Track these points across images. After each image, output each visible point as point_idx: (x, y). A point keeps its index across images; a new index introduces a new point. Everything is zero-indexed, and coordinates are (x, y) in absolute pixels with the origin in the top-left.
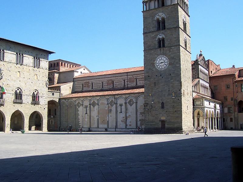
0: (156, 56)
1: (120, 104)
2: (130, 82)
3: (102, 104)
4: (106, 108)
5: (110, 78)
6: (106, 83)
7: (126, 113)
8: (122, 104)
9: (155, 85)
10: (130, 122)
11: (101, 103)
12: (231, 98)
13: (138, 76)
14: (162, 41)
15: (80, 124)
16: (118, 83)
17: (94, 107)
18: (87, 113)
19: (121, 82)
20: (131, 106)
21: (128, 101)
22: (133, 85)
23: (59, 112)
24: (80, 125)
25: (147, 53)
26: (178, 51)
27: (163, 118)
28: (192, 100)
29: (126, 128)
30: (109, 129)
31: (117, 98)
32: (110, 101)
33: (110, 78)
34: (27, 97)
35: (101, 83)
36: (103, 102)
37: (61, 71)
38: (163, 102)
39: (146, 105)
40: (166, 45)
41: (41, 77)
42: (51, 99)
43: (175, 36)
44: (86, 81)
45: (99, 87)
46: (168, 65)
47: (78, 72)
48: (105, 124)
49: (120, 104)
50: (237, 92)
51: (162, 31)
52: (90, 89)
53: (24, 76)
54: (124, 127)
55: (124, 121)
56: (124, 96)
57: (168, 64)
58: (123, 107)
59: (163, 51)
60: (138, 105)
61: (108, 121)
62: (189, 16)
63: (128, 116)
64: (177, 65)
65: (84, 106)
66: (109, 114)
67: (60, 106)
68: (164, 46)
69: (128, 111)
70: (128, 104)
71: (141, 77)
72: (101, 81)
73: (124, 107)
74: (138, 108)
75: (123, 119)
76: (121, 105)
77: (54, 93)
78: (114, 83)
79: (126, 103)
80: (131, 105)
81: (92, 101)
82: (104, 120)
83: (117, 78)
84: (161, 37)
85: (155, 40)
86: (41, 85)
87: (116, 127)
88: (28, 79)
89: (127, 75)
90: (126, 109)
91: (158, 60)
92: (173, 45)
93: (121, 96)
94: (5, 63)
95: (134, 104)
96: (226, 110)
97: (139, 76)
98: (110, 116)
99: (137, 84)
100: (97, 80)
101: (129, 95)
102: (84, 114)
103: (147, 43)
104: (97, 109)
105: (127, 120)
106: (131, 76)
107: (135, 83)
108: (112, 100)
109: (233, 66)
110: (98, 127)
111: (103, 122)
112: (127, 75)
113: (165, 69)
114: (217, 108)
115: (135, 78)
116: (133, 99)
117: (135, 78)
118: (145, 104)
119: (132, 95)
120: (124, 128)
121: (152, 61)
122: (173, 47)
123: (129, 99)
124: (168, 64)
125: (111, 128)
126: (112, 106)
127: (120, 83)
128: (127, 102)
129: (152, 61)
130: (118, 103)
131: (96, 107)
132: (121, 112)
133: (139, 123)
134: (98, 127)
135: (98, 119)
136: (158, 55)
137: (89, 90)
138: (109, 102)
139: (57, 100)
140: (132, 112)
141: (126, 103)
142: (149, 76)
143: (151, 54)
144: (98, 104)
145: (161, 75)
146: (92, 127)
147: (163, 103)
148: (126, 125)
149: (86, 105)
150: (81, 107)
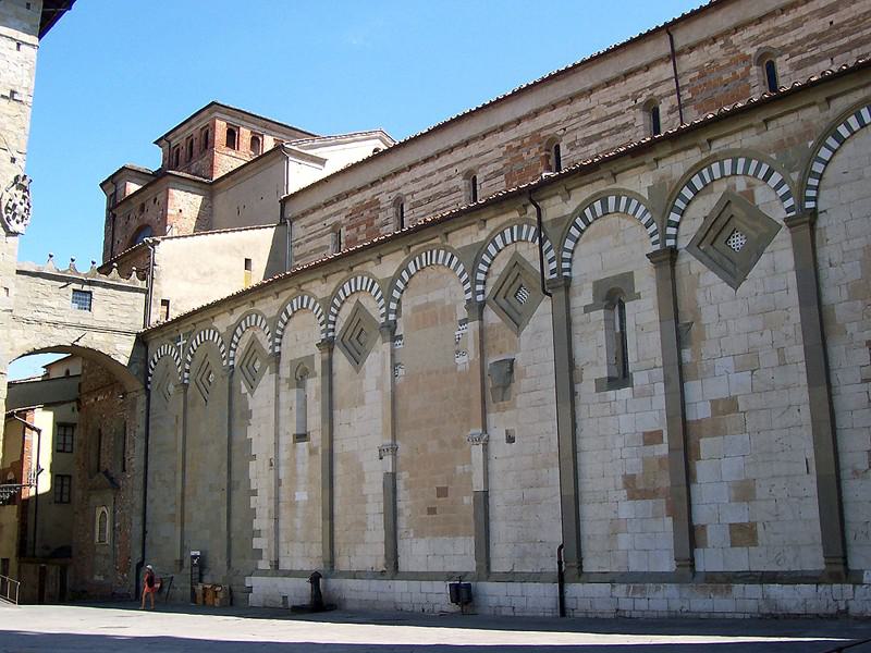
1: (597, 285)
3: (431, 316)
5: (528, 127)
7: (679, 375)
8: (628, 278)
10: (745, 492)
11: (416, 309)
17: (357, 359)
18: (301, 437)
19: (625, 127)
21: (691, 226)
23: (140, 444)
24: (257, 543)
30: (493, 593)
31: (566, 223)
32: (499, 267)
33: (528, 127)
35: (459, 182)
36: (434, 296)
42: (66, 337)
44: (358, 198)
48: (454, 533)
49: (597, 285)
54: (667, 565)
55: (664, 482)
56: (639, 181)
58: (643, 313)
60: (827, 253)
61: (484, 499)
63: (699, 411)
65: (285, 371)
66: (492, 417)
67: (148, 392)
69: (709, 349)
70: (689, 264)
73: (654, 316)
74: (831, 295)
75: (645, 461)
76: (614, 296)
77: (97, 290)
78: (564, 151)
79: (674, 251)
80: (734, 271)
81: (347, 310)
82: (442, 492)
83: (581, 105)
87: (570, 565)
90: (680, 330)
93: (601, 186)
95: (781, 255)
97: (797, 24)
98: (497, 434)
101: (694, 156)
102: (286, 440)
104: (380, 386)
105: (702, 469)
106: (716, 51)
108: (517, 264)
111: (435, 514)
112: (674, 56)
116: (749, 194)
117: (751, 51)
119: (747, 139)
120: (661, 578)
123: (703, 208)
125: (510, 577)
126: (516, 320)
128: (683, 243)
130: (574, 274)
131: (378, 355)
132: (620, 377)
134: (392, 568)
135: (391, 484)
138: (492, 281)
139: (121, 350)
140: (749, 362)
141: (666, 258)
144: (390, 331)
146: (343, 563)
148: (692, 536)
149: (298, 355)
150: (267, 383)
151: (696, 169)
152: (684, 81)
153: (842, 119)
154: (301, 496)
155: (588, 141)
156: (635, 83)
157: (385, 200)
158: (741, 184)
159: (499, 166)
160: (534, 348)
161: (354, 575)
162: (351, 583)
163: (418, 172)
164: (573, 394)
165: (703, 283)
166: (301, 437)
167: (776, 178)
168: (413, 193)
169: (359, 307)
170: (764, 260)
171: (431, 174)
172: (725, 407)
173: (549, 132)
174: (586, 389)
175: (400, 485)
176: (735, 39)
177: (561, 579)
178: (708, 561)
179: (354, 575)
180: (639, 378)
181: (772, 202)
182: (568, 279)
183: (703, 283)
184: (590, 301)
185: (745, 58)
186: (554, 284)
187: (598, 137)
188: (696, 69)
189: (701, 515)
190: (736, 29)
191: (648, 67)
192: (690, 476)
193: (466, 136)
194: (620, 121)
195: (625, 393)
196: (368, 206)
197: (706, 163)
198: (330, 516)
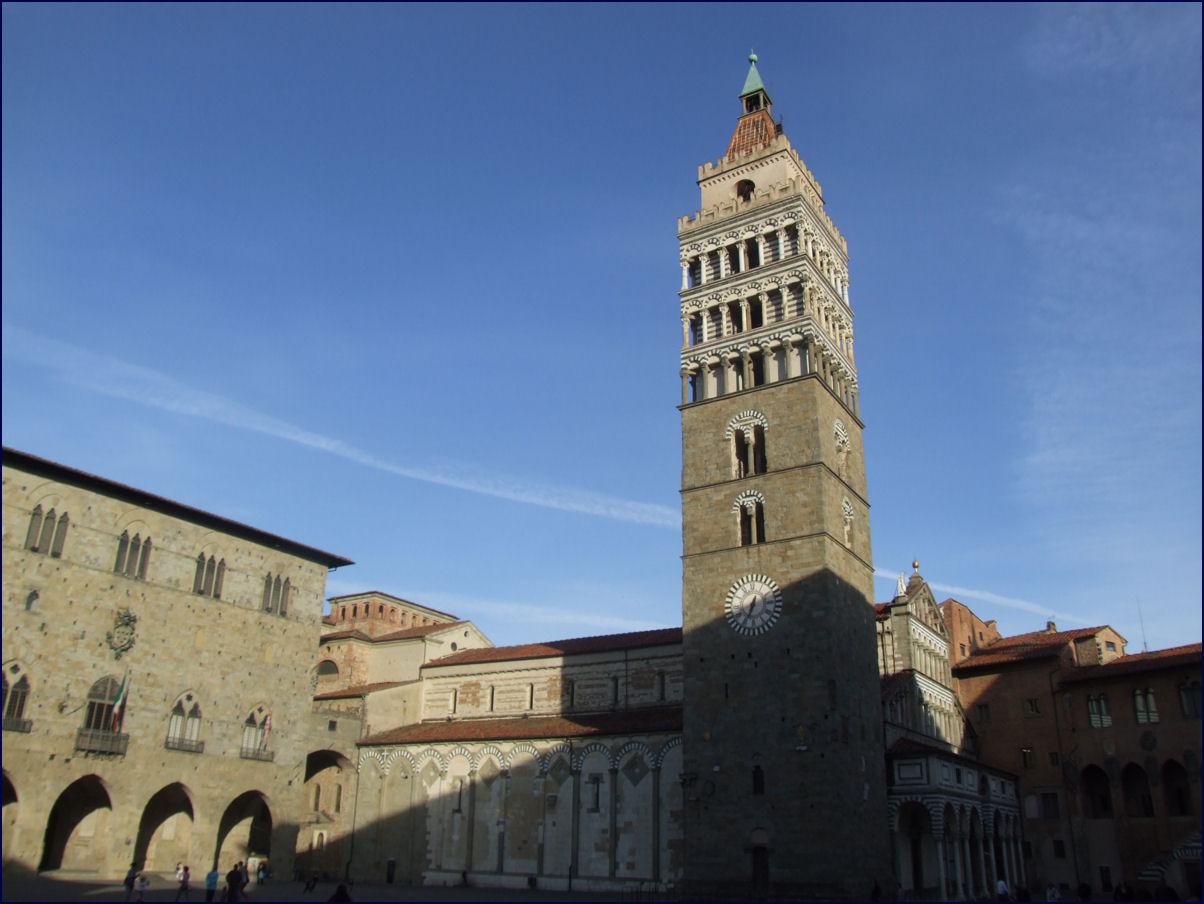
0: (729, 578)
1: (590, 775)
2: (638, 687)
4: (536, 792)
6: (544, 689)
7: (615, 812)
8: (602, 774)
9: (727, 696)
12: (1051, 754)
13: (667, 665)
14: (754, 520)
15: (430, 852)
16: (589, 690)
18: (459, 811)
19: (604, 685)
20: (635, 785)
21: (621, 765)
22: (647, 699)
24: (429, 856)
25: (693, 565)
26: (819, 558)
27: (760, 839)
28: (883, 761)
29: (613, 874)
34: (224, 731)
37: (377, 635)
38: (758, 767)
39: (688, 780)
40: (769, 534)
41: (288, 652)
43: (806, 498)
44: (468, 679)
45: (517, 705)
46: (778, 615)
47: (442, 643)
49: (590, 775)
50: (1074, 730)
51: (753, 482)
52: (483, 710)
53: (222, 646)
54: (607, 875)
55: (608, 845)
57: (779, 609)
58: (605, 788)
59: (759, 556)
61: (541, 847)
62: (862, 426)
63: (620, 825)
64: (815, 614)
66: (548, 816)
68: (761, 539)
70: (622, 776)
71: (680, 667)
72: (526, 680)
74: (663, 795)
76: (596, 779)
78: (576, 688)
80: (636, 780)
81: (484, 760)
82: (525, 842)
84: (750, 503)
85: (726, 513)
86: (285, 686)
87: (573, 872)
88: (234, 660)
89: (626, 661)
90: (616, 797)
91: (740, 593)
92: (798, 534)
93: (594, 741)
94: (148, 592)
95: (649, 779)
96: (1032, 806)
99: (666, 696)
100: (510, 675)
101: (627, 740)
103: (696, 526)
104: (500, 794)
105: (619, 844)
106: (643, 664)
107: (655, 692)
109: (1050, 625)
110: (500, 870)
113: (767, 628)
114: (992, 798)
115: (656, 669)
116: (642, 757)
118: (685, 774)
120: (604, 879)
121: (716, 600)
122: (798, 542)
123: (628, 757)
124: (779, 609)
125: (550, 876)
126: (560, 782)
127: (595, 690)
129: (716, 600)
130: (583, 769)
132: (596, 809)
133: (666, 856)
134: (500, 870)
135: (501, 837)
136: (739, 573)
137: (479, 715)
141: (614, 772)
142: (702, 660)
143: (711, 570)
145: (750, 655)
146: (476, 867)
147: (758, 774)
148: (615, 866)
151: (627, 744)
152: (630, 673)
153: (670, 741)
154: (456, 837)
155: (588, 687)
156: (611, 667)
157: (484, 684)
158: (640, 753)
159: (545, 686)
160: (565, 792)
161: (484, 873)
162: (481, 876)
163: (503, 676)
164: (579, 813)
165: (626, 783)
166: (459, 811)
167: (650, 754)
168: (500, 686)
169: (490, 760)
170: (644, 780)
171: (510, 679)
172: (629, 824)
173: (570, 677)
174: (583, 811)
175: (506, 838)
176: (651, 662)
177: (570, 877)
178: (622, 871)
179: (484, 873)
180: (602, 810)
181: (648, 760)
182: (580, 772)
183: (626, 783)
184: (587, 780)
185: (654, 671)
186: (576, 771)
187: (592, 686)
188: (636, 669)
189: (618, 860)
190: (653, 658)
191: (615, 662)
192: (616, 845)
193: (530, 667)
194: (602, 682)
195: (597, 815)
196: (473, 685)
197: (630, 743)
198: (470, 847)
